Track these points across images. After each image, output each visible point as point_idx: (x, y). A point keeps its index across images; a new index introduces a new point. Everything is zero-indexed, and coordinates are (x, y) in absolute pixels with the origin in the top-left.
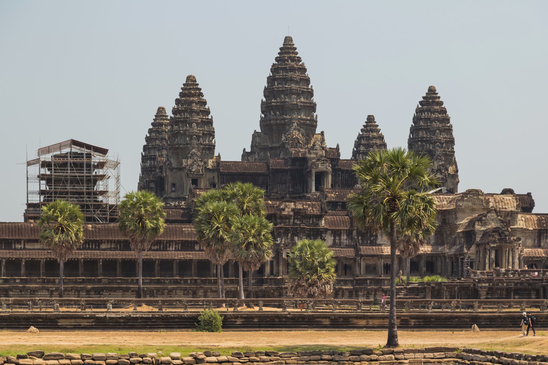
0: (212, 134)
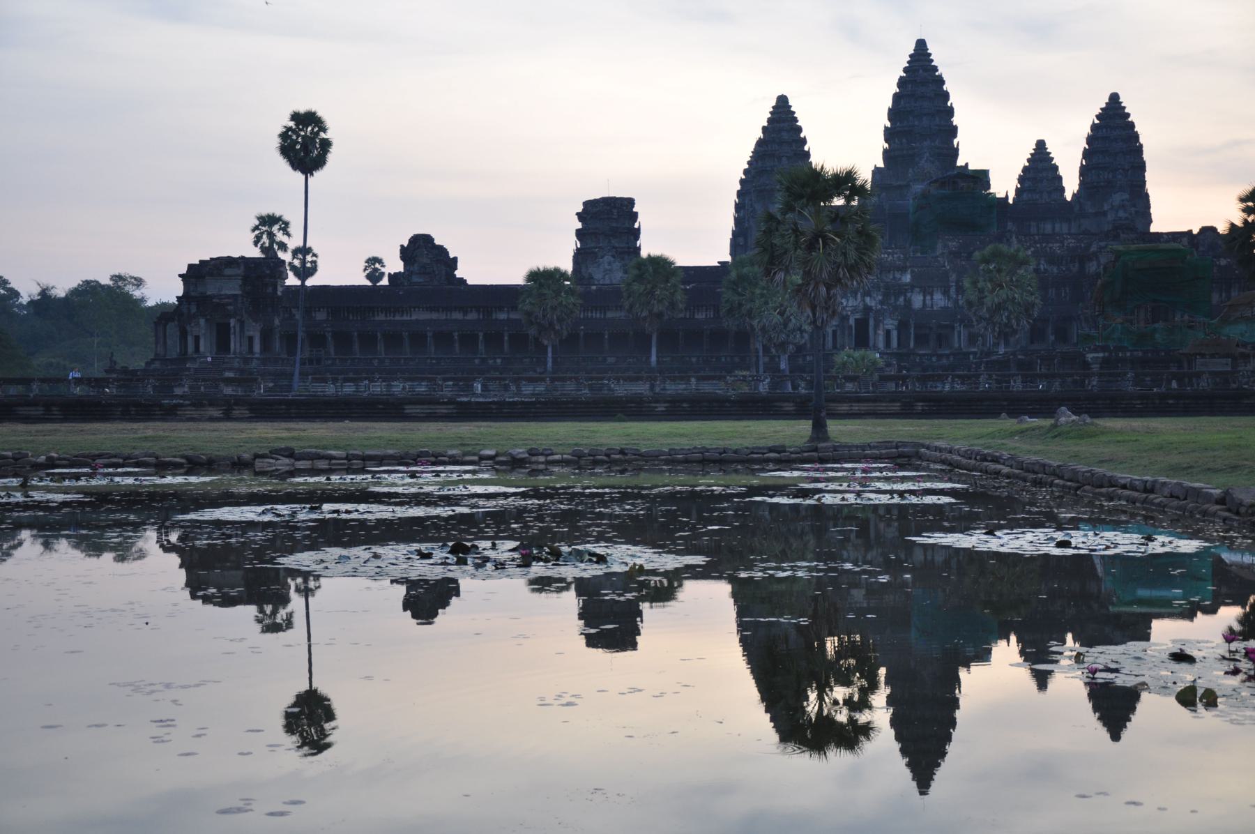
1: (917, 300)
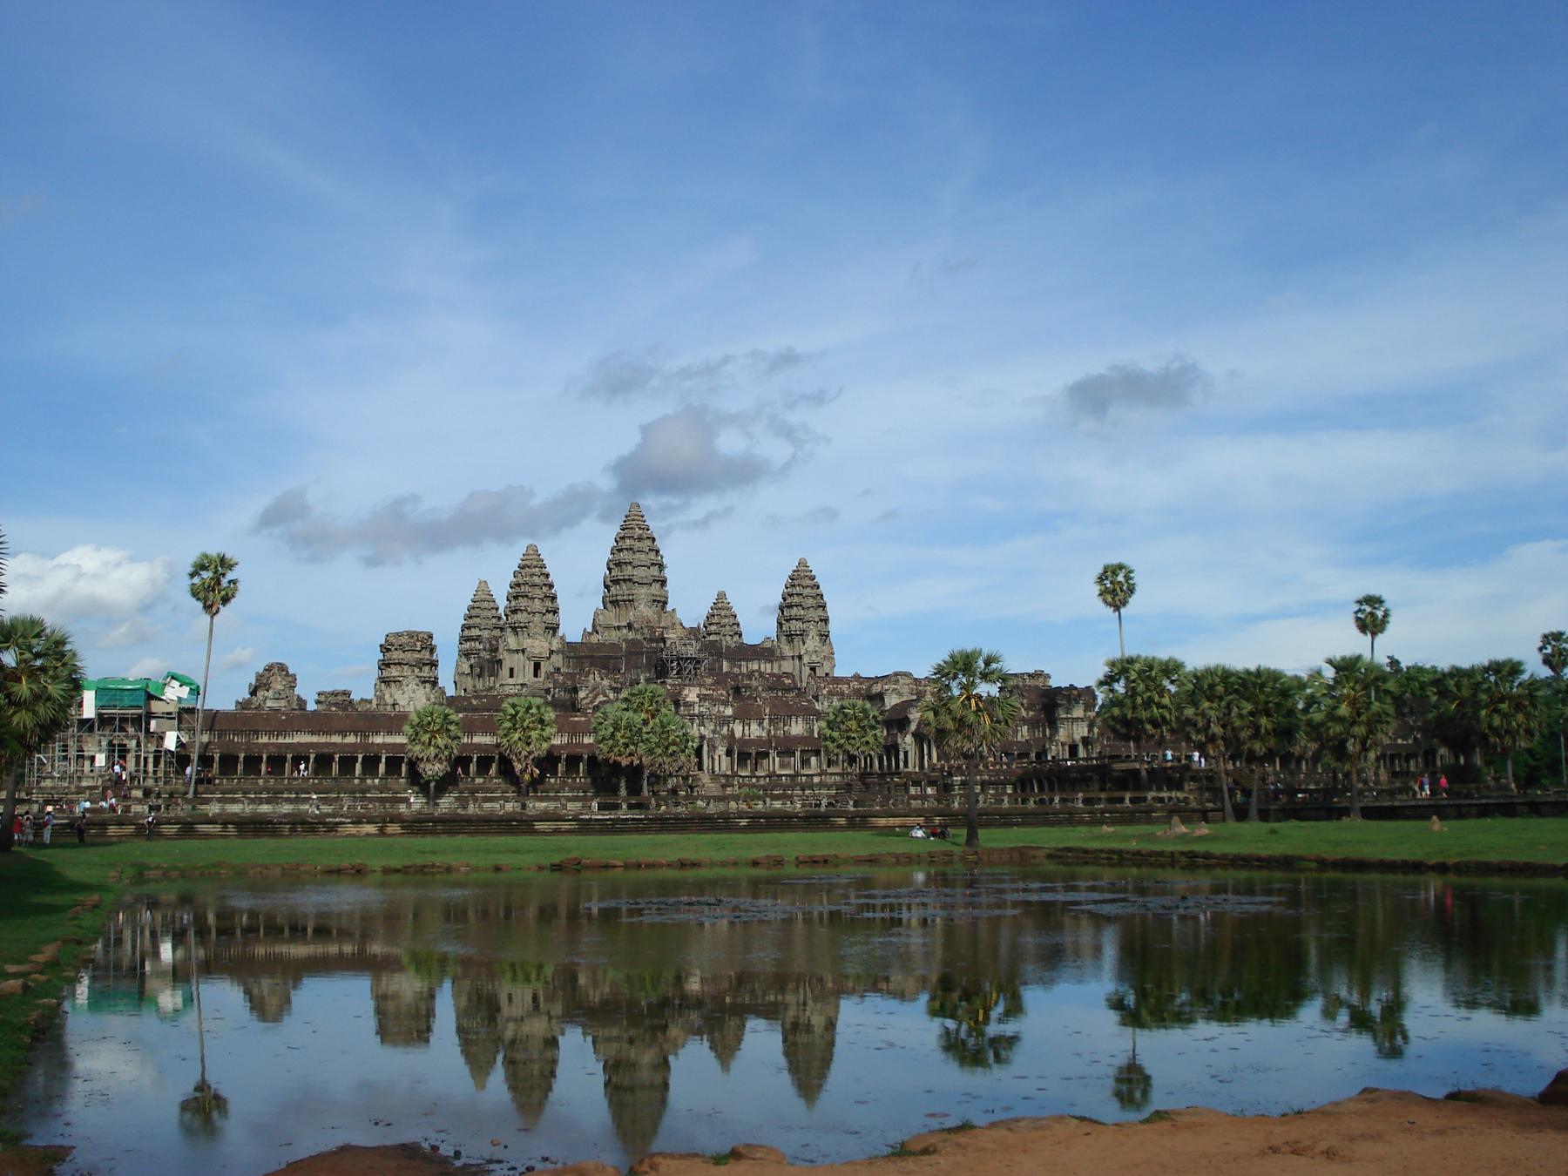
0: (555, 612)
1: (738, 729)
